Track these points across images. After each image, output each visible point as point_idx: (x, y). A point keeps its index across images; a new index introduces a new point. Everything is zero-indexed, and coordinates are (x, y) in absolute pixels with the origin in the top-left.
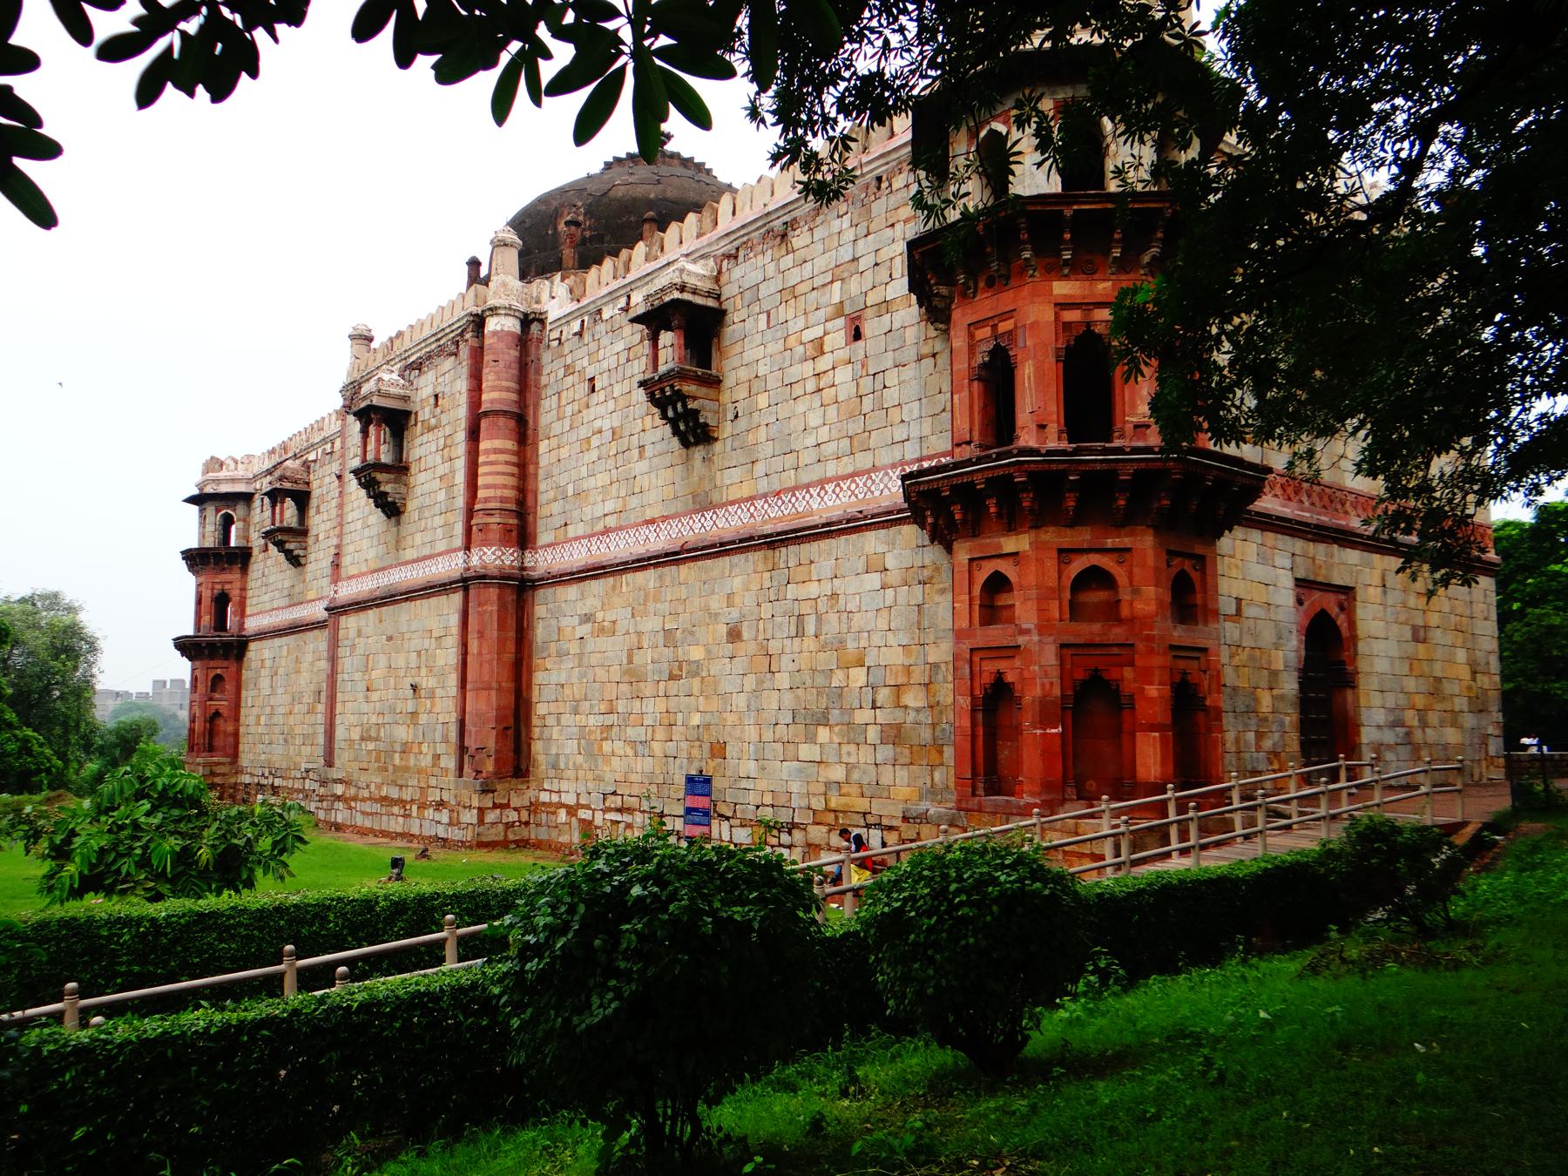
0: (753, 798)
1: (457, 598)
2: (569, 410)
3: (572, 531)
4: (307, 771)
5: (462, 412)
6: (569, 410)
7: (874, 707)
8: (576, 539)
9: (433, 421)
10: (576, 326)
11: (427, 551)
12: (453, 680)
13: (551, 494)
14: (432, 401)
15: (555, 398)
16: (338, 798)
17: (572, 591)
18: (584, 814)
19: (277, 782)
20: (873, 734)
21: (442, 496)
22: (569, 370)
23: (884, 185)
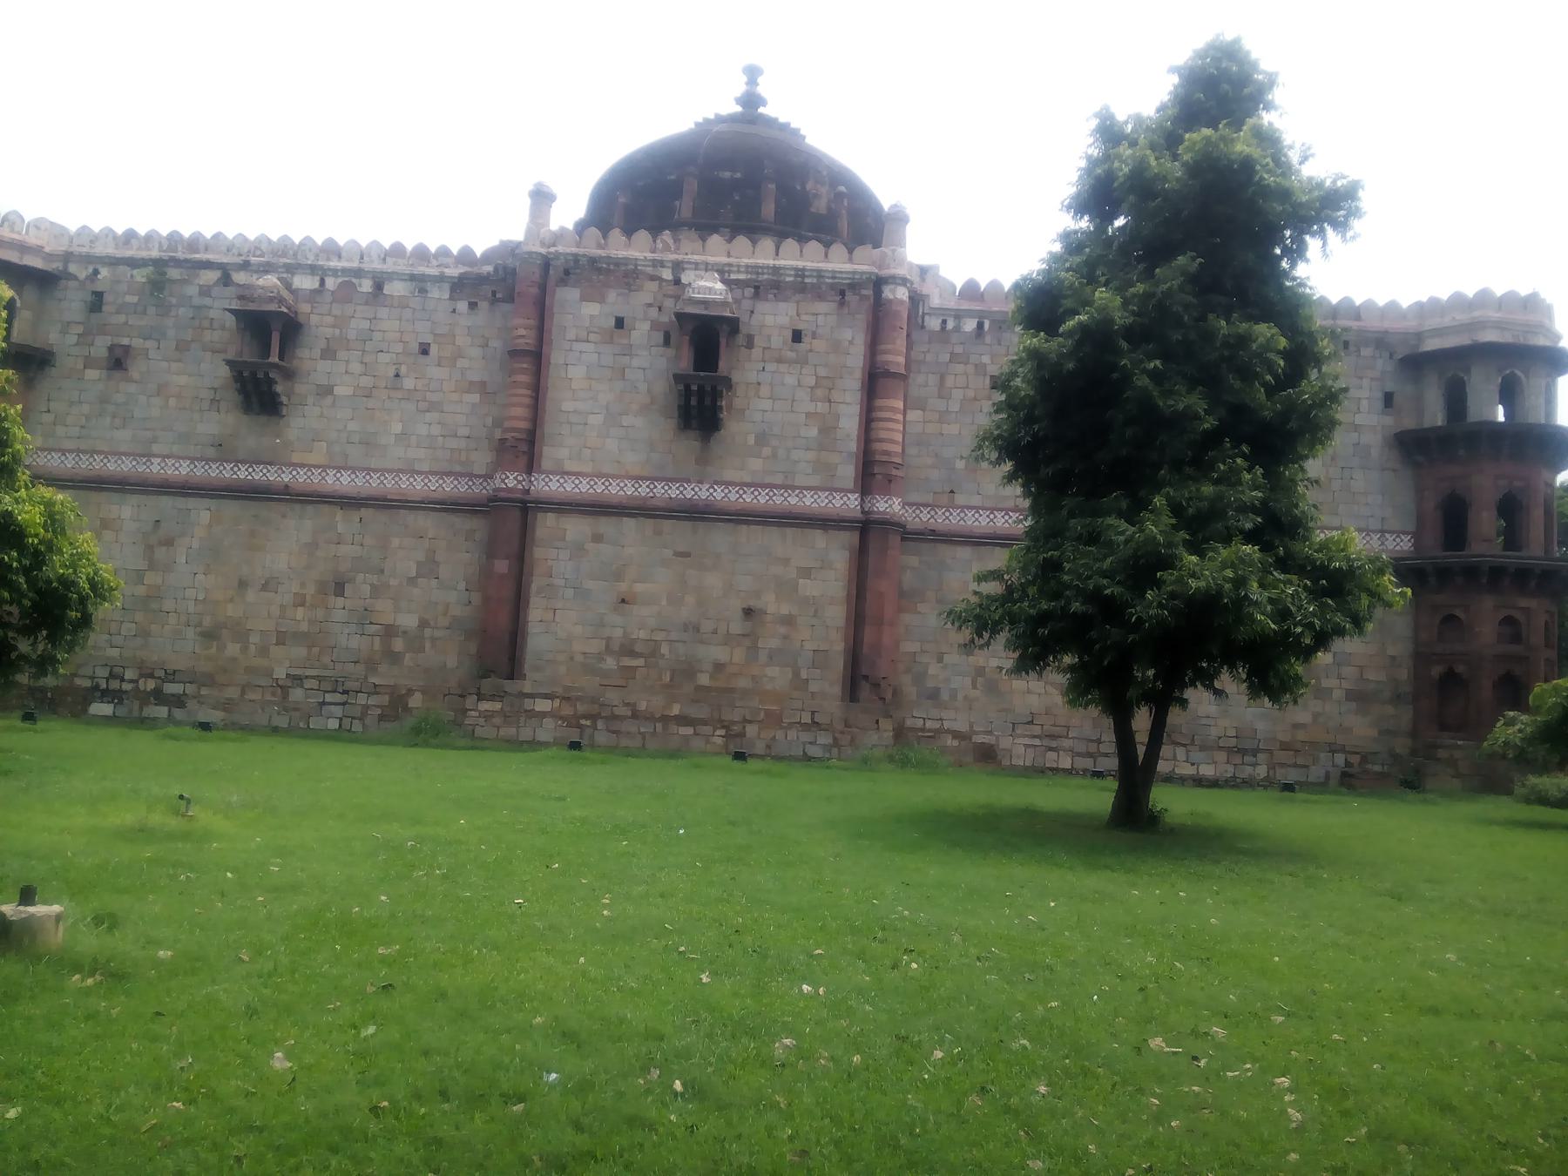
0: (1214, 732)
1: (852, 538)
2: (957, 394)
3: (960, 499)
4: (298, 680)
5: (856, 359)
6: (957, 394)
7: (1339, 677)
8: (970, 508)
9: (791, 355)
10: (970, 325)
11: (778, 480)
12: (836, 615)
13: (930, 461)
14: (789, 335)
15: (933, 380)
16: (543, 715)
17: (964, 553)
18: (979, 739)
19: (171, 688)
20: (1337, 694)
21: (814, 432)
22: (954, 358)
23: (1352, 348)
